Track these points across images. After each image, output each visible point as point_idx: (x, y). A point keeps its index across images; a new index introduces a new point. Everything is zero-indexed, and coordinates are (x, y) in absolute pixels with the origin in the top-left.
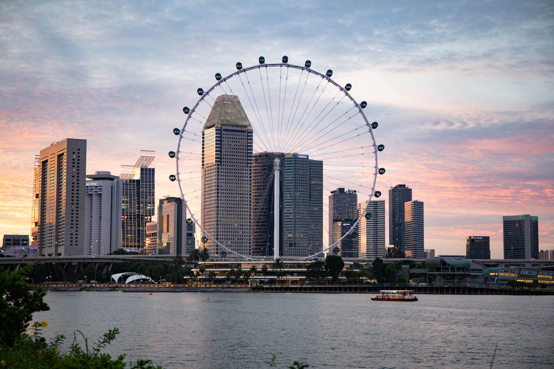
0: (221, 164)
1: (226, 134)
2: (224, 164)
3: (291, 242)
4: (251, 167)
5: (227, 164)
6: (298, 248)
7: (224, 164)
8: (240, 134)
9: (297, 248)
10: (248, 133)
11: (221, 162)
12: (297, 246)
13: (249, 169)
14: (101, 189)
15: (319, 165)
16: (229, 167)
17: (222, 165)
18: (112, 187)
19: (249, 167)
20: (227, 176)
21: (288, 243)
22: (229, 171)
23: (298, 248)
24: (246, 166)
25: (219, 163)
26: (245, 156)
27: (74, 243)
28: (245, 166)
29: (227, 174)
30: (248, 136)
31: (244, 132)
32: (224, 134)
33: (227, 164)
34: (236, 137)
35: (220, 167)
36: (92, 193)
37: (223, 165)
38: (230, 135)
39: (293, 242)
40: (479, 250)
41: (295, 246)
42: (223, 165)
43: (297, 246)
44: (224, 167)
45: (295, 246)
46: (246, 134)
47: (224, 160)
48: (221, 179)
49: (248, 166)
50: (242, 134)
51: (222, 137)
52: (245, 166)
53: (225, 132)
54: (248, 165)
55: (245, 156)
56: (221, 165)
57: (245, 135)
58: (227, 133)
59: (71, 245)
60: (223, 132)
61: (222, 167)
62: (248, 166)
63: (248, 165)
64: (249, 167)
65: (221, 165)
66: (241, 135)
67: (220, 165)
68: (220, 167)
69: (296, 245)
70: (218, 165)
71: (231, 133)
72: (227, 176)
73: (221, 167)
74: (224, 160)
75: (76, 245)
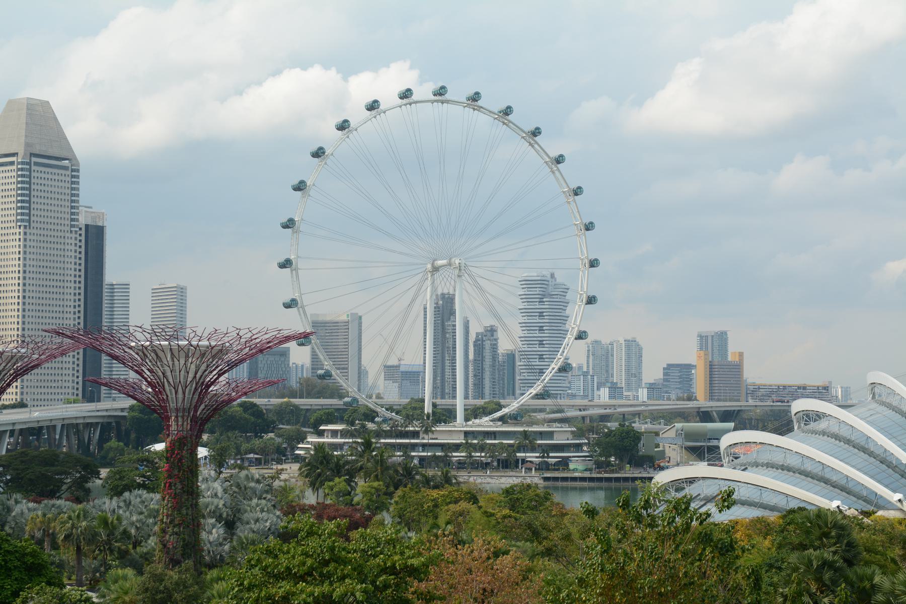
5: (39, 225)
8: (60, 171)
10: (73, 171)
11: (29, 221)
13: (73, 235)
17: (32, 228)
25: (27, 224)
28: (68, 231)
29: (39, 245)
30: (73, 177)
33: (39, 225)
35: (28, 231)
37: (33, 228)
38: (45, 172)
40: (273, 369)
42: (33, 228)
44: (35, 231)
46: (69, 173)
49: (71, 232)
50: (63, 172)
54: (72, 229)
56: (30, 228)
57: (68, 175)
60: (33, 168)
62: (71, 232)
63: (72, 229)
64: (74, 232)
65: (30, 228)
67: (28, 227)
70: (25, 227)
71: (43, 169)
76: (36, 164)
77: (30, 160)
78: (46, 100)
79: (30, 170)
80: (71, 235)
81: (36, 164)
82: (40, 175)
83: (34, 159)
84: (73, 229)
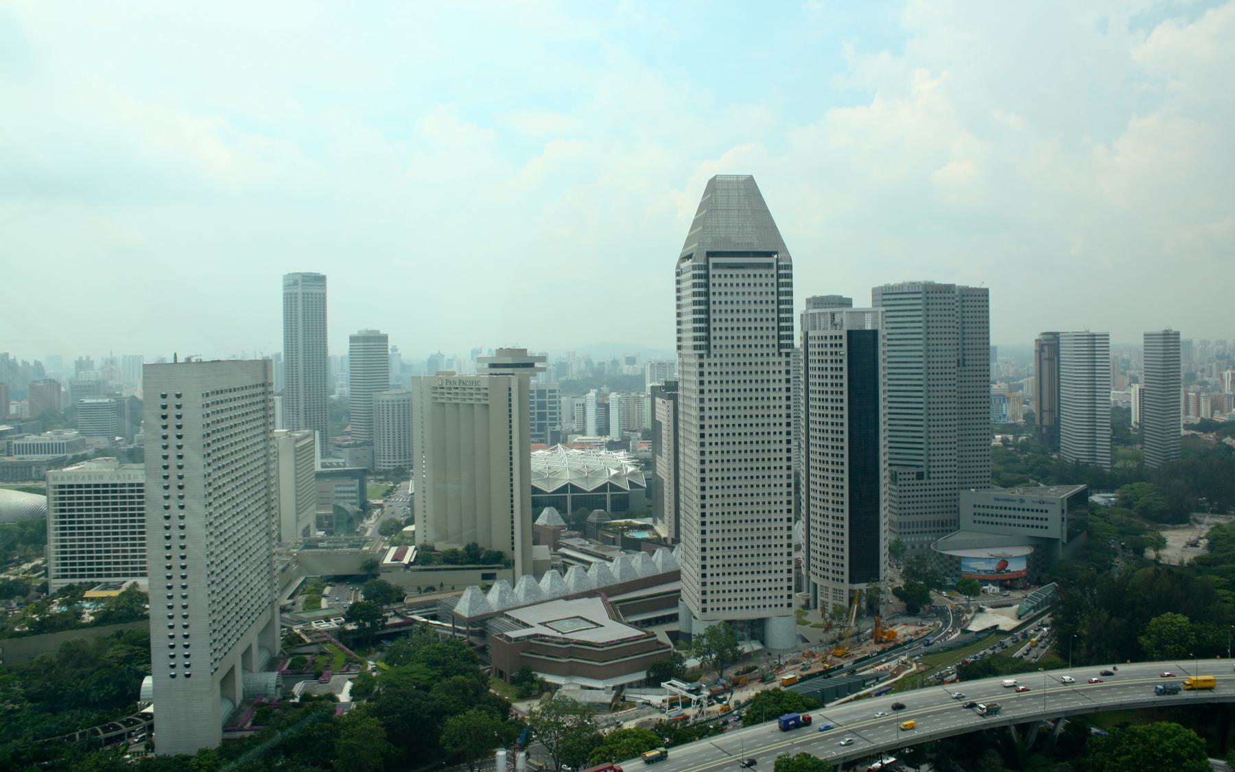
0: (709, 352)
1: (720, 276)
2: (718, 351)
3: (920, 470)
7: (718, 351)
9: (932, 481)
10: (779, 268)
11: (708, 347)
12: (934, 478)
13: (784, 359)
14: (487, 395)
15: (981, 298)
17: (712, 355)
20: (724, 382)
21: (913, 473)
23: (936, 481)
24: (777, 354)
26: (773, 328)
27: (180, 671)
28: (774, 354)
31: (770, 266)
32: (714, 276)
34: (747, 281)
35: (705, 361)
37: (715, 356)
39: (924, 470)
41: (929, 478)
42: (715, 356)
43: (934, 478)
44: (718, 360)
45: (929, 478)
48: (710, 391)
49: (780, 354)
50: (763, 272)
52: (774, 354)
53: (717, 272)
55: (773, 328)
57: (772, 276)
58: (723, 272)
59: (173, 676)
60: (712, 272)
61: (712, 360)
64: (784, 355)
65: (709, 356)
66: (761, 276)
67: (705, 356)
69: (932, 475)
70: (701, 356)
72: (724, 382)
73: (709, 361)
75: (188, 676)
76: (716, 266)
77: (708, 262)
78: (749, 174)
80: (780, 359)
81: (716, 266)
82: (723, 281)
83: (712, 260)
84: (783, 351)
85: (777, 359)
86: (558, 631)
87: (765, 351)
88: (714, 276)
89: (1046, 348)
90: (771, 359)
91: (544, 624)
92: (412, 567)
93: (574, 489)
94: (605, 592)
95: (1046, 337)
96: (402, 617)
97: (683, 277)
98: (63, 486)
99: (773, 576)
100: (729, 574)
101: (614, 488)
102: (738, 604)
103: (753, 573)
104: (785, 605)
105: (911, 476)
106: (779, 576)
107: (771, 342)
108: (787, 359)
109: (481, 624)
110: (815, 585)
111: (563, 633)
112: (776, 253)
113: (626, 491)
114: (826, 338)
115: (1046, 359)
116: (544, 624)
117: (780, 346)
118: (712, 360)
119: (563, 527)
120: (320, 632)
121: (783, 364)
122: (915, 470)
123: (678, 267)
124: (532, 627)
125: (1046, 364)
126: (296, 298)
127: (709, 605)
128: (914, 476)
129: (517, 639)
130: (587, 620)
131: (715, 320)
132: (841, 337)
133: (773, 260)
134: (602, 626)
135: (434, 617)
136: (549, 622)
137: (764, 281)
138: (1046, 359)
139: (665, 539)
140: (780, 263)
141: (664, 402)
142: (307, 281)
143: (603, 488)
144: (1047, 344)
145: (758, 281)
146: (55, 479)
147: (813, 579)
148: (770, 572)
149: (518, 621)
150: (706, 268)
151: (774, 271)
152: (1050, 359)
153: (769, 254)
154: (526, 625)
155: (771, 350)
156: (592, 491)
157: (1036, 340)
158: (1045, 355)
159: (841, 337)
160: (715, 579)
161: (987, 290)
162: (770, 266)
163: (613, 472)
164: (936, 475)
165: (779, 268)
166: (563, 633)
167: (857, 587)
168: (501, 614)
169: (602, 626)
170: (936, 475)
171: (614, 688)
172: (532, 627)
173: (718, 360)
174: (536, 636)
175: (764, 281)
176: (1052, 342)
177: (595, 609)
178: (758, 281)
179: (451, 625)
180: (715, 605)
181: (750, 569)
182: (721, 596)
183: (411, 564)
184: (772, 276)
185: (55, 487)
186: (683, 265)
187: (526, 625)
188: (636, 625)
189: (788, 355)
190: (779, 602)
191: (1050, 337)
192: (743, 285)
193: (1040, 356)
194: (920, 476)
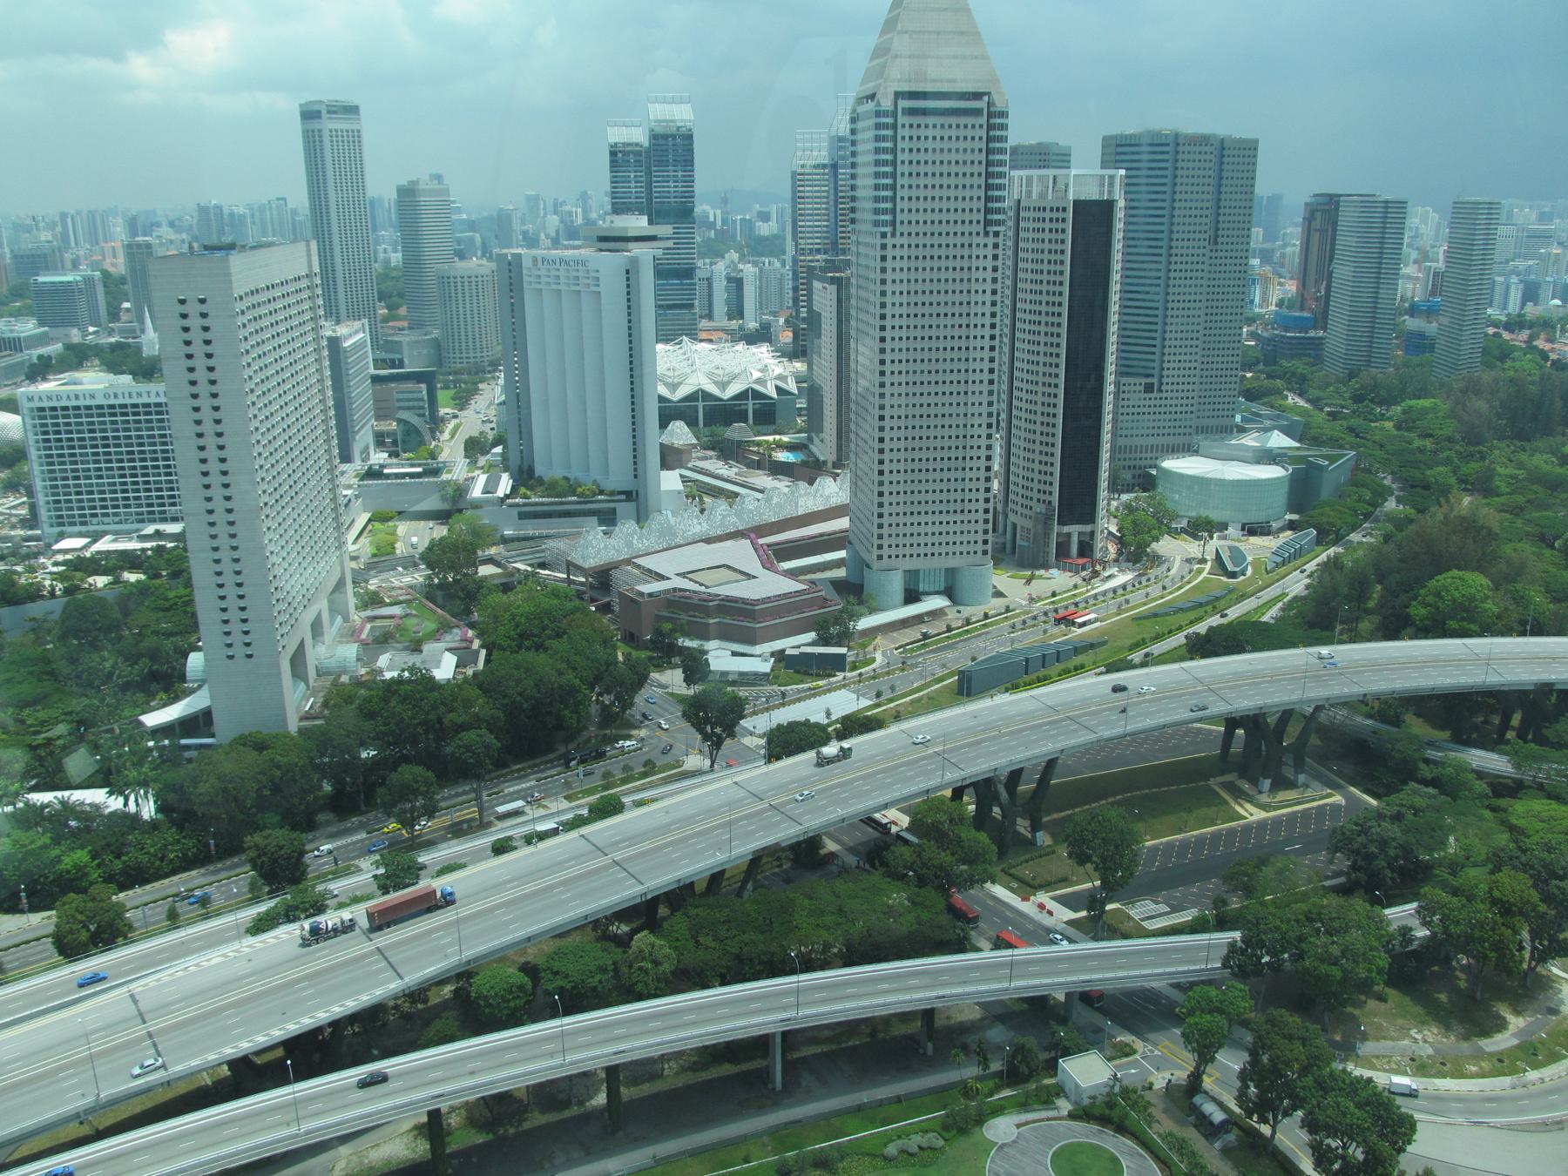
0: (895, 229)
2: (905, 229)
3: (1149, 380)
4: (996, 234)
6: (1169, 395)
7: (905, 229)
9: (1164, 395)
11: (893, 223)
15: (1247, 153)
16: (921, 240)
17: (898, 234)
18: (628, 272)
19: (991, 234)
22: (920, 252)
23: (1169, 395)
25: (888, 229)
27: (239, 650)
28: (978, 234)
29: (913, 264)
31: (977, 112)
35: (889, 241)
36: (578, 288)
37: (902, 234)
39: (1155, 380)
41: (1160, 391)
42: (902, 234)
44: (905, 241)
45: (1160, 391)
47: (905, 217)
48: (894, 281)
49: (986, 234)
50: (970, 121)
51: (899, 138)
52: (978, 234)
54: (988, 228)
56: (893, 235)
57: (981, 126)
59: (231, 657)
60: (900, 120)
61: (898, 241)
64: (991, 234)
65: (893, 235)
68: (889, 241)
70: (884, 235)
73: (894, 241)
74: (905, 217)
75: (250, 656)
79: (894, 126)
80: (986, 240)
83: (903, 104)
85: (981, 240)
86: (701, 585)
87: (967, 228)
88: (903, 126)
89: (1318, 215)
90: (976, 240)
91: (683, 575)
92: (509, 501)
93: (707, 396)
94: (753, 533)
95: (1320, 199)
96: (498, 564)
97: (860, 125)
98: (43, 409)
99: (966, 517)
100: (912, 513)
101: (757, 395)
102: (922, 550)
103: (941, 512)
104: (980, 553)
105: (1138, 388)
106: (973, 517)
107: (975, 217)
108: (996, 240)
109: (603, 578)
110: (1015, 526)
111: (707, 587)
112: (989, 94)
113: (771, 398)
114: (1044, 209)
115: (1316, 230)
116: (683, 575)
117: (987, 223)
118: (898, 241)
119: (694, 446)
120: (401, 588)
121: (990, 246)
122: (1144, 381)
123: (854, 111)
124: (668, 579)
125: (1316, 237)
126: (320, 136)
127: (885, 552)
128: (1142, 388)
129: (650, 595)
130: (735, 570)
131: (903, 186)
132: (1064, 210)
133: (981, 104)
134: (754, 577)
135: (543, 566)
136: (689, 573)
137: (969, 133)
138: (1316, 230)
139: (825, 462)
140: (992, 109)
141: (824, 288)
142: (335, 112)
143: (743, 396)
144: (1322, 210)
145: (962, 133)
146: (31, 399)
147: (1012, 518)
148: (962, 511)
149: (650, 571)
150: (894, 114)
151: (983, 120)
152: (1322, 231)
153: (977, 96)
154: (662, 577)
155: (975, 228)
156: (729, 400)
157: (1306, 204)
158: (1317, 224)
159: (1064, 210)
160: (894, 520)
161: (1256, 141)
162: (977, 112)
163: (757, 375)
164: (1170, 387)
165: (990, 115)
166: (707, 587)
167: (1066, 529)
168: (628, 562)
169: (754, 577)
170: (1170, 387)
171: (772, 654)
172: (668, 579)
173: (905, 241)
174: (675, 590)
175: (969, 133)
176: (1326, 207)
177: (742, 554)
178: (962, 133)
179: (565, 576)
180: (893, 552)
181: (937, 507)
182: (901, 541)
183: (507, 497)
184: (981, 126)
185: (32, 410)
186: (861, 109)
187: (662, 577)
188: (793, 574)
189: (996, 234)
190: (972, 548)
191: (1325, 200)
192: (942, 138)
193: (1310, 223)
194: (1149, 388)
